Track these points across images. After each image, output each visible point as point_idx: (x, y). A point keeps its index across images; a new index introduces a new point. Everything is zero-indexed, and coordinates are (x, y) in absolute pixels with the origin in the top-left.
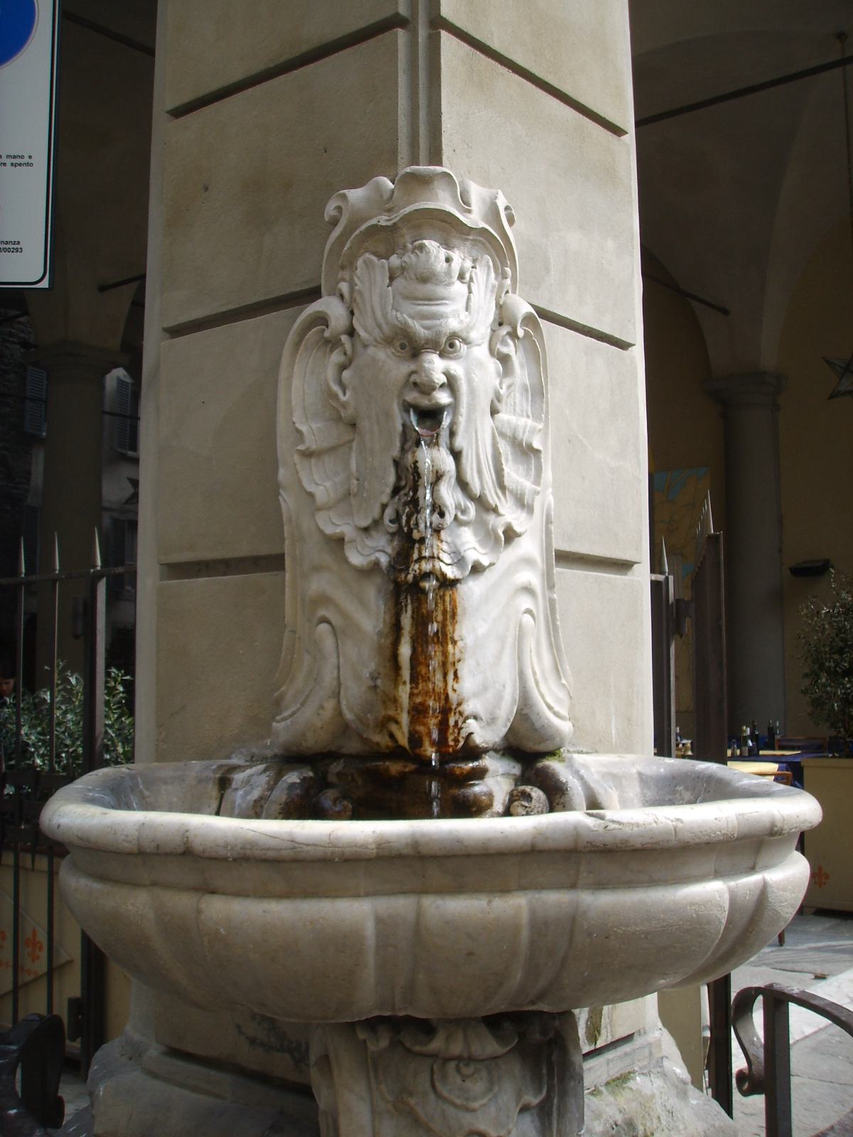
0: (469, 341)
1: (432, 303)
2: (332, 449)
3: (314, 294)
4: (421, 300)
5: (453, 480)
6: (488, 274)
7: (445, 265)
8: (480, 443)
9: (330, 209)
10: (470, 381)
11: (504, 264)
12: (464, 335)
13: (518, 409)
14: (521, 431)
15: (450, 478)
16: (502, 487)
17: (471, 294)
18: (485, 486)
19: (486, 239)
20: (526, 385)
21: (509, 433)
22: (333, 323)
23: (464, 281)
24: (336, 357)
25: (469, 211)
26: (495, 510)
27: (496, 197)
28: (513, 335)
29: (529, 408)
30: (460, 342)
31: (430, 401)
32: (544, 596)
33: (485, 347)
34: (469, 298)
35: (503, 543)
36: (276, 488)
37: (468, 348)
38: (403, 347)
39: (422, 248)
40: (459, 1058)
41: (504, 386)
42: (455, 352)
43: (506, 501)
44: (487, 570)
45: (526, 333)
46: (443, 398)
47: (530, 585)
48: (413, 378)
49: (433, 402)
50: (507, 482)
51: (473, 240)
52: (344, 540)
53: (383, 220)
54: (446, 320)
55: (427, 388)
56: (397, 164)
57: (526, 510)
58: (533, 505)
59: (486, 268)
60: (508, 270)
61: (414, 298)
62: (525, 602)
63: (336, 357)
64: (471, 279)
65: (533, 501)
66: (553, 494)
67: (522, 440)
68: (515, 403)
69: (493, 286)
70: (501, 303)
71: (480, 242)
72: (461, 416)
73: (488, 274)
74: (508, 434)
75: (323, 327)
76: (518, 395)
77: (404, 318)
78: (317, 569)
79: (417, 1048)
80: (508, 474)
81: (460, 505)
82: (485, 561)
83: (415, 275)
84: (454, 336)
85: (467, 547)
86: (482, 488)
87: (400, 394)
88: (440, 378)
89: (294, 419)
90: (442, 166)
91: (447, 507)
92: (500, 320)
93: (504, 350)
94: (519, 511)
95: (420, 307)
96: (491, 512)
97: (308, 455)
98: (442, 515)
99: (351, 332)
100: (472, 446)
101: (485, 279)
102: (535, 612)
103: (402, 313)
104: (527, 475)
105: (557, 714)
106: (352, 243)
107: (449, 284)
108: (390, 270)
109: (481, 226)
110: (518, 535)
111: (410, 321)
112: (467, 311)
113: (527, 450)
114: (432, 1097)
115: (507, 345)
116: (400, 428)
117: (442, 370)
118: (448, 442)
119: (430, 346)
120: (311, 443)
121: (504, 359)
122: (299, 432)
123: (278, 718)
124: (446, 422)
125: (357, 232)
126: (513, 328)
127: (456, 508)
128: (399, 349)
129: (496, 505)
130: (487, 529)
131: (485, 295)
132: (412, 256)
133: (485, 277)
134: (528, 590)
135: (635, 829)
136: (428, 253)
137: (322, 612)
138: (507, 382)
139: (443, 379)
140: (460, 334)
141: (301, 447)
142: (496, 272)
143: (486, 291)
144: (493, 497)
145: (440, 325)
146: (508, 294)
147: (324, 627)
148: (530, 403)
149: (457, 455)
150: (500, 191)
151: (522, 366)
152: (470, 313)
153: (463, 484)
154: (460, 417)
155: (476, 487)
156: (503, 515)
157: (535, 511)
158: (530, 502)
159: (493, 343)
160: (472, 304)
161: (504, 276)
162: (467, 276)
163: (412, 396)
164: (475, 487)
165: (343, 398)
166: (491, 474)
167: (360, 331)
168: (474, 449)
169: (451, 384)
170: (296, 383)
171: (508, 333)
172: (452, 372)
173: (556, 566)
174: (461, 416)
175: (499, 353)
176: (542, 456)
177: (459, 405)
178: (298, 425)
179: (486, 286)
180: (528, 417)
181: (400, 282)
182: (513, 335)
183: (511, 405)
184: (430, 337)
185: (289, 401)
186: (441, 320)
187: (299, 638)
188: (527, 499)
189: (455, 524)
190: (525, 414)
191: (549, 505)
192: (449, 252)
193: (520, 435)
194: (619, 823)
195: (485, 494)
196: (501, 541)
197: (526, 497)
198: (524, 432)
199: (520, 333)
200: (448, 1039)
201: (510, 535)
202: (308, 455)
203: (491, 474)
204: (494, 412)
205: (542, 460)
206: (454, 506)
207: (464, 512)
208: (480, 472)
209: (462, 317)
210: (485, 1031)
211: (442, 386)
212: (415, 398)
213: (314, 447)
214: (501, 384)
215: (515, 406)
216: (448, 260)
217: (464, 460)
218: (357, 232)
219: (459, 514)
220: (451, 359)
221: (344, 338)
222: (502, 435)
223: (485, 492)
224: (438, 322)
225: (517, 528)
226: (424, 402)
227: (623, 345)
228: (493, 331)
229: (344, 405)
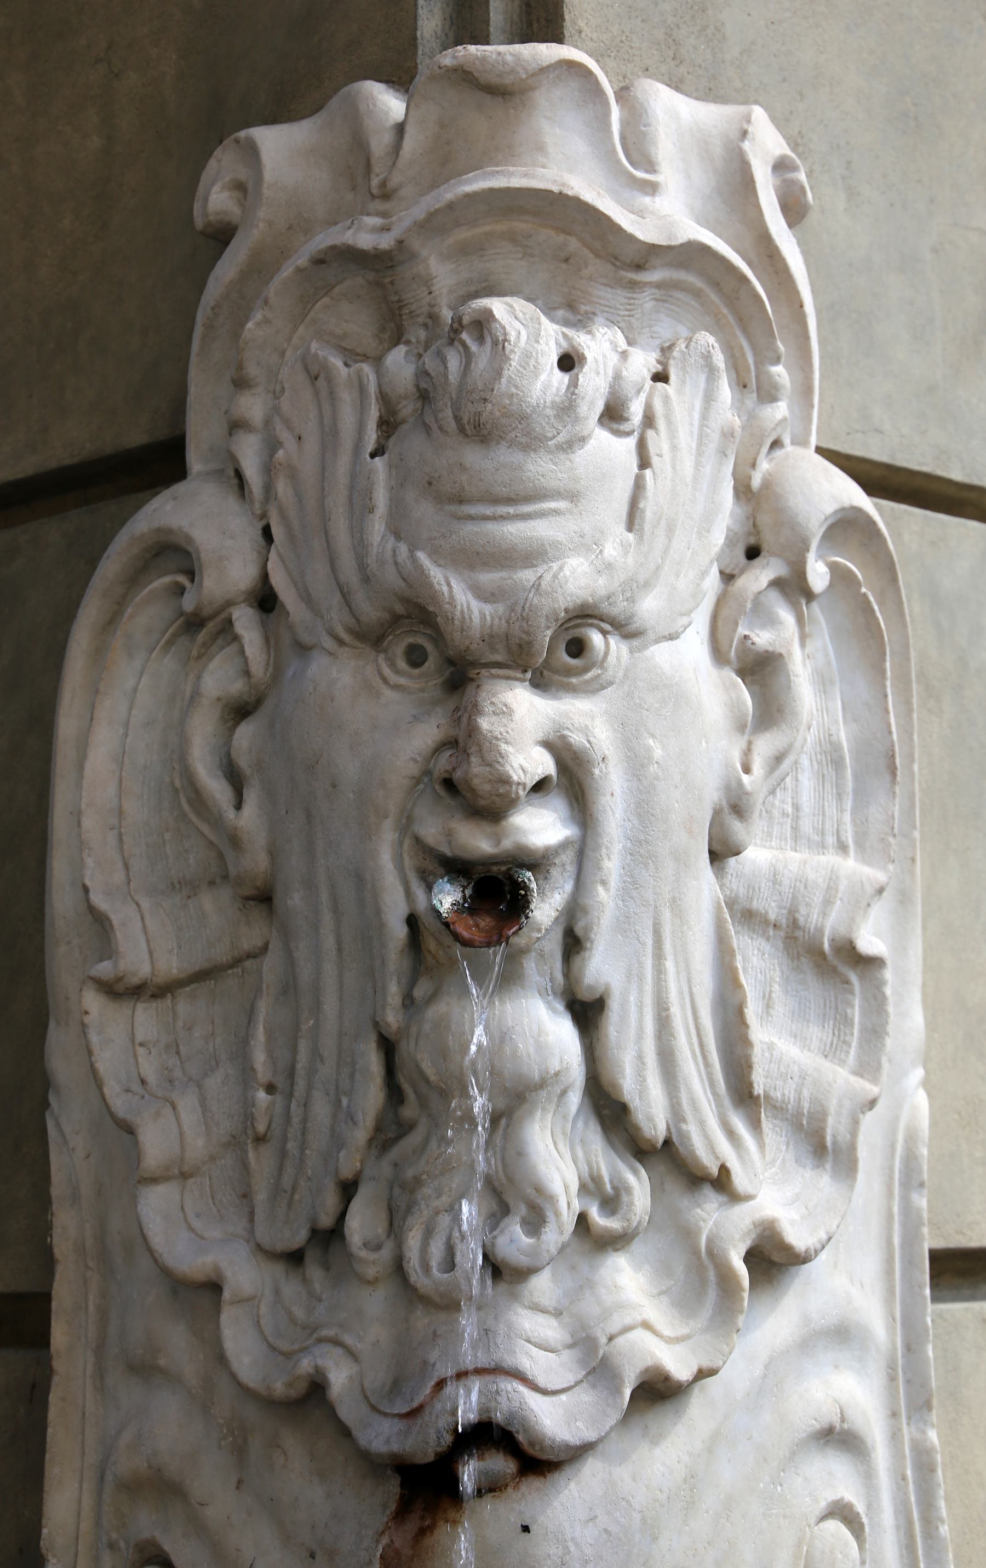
0: (633, 627)
1: (511, 510)
5: (575, 1099)
6: (709, 397)
7: (560, 379)
8: (669, 965)
11: (767, 355)
12: (618, 608)
13: (806, 825)
14: (818, 899)
15: (564, 1093)
17: (648, 472)
19: (702, 274)
20: (835, 748)
21: (773, 910)
23: (625, 427)
25: (652, 188)
27: (744, 133)
29: (847, 817)
30: (604, 633)
32: (895, 1436)
34: (639, 486)
35: (746, 1295)
37: (631, 651)
41: (758, 767)
42: (586, 669)
43: (761, 1145)
44: (696, 1389)
45: (834, 569)
47: (843, 1420)
49: (507, 844)
50: (760, 1083)
51: (660, 285)
54: (555, 566)
57: (828, 1166)
58: (853, 1147)
59: (702, 379)
60: (779, 371)
64: (649, 421)
65: (854, 1133)
66: (926, 1084)
67: (820, 931)
68: (797, 807)
69: (724, 435)
70: (756, 482)
72: (604, 883)
73: (709, 397)
74: (772, 916)
76: (807, 782)
77: (414, 560)
80: (771, 1047)
81: (596, 1179)
82: (681, 1371)
83: (457, 419)
85: (614, 1325)
86: (676, 1114)
87: (406, 824)
90: (557, 37)
91: (552, 1199)
92: (752, 540)
93: (763, 639)
94: (808, 1173)
96: (708, 1191)
98: (535, 1222)
100: (641, 978)
101: (696, 416)
102: (860, 1508)
104: (832, 1052)
107: (571, 445)
111: (436, 574)
112: (630, 527)
113: (836, 962)
115: (771, 621)
117: (540, 736)
118: (559, 977)
119: (499, 658)
126: (790, 564)
128: (402, 664)
129: (724, 1170)
130: (695, 1252)
131: (698, 465)
133: (698, 404)
136: (499, 346)
138: (765, 745)
139: (543, 764)
140: (605, 608)
142: (741, 384)
143: (700, 453)
145: (537, 586)
146: (778, 453)
148: (849, 804)
150: (758, 113)
151: (822, 682)
152: (641, 538)
154: (600, 889)
156: (749, 1198)
157: (861, 1165)
158: (844, 1137)
159: (725, 613)
160: (649, 507)
161: (768, 394)
162: (636, 410)
164: (650, 1119)
166: (707, 1064)
168: (649, 987)
171: (777, 583)
172: (576, 739)
173: (935, 1299)
174: (604, 883)
176: (888, 974)
177: (597, 848)
179: (702, 439)
180: (842, 848)
183: (785, 815)
186: (540, 570)
188: (835, 1127)
190: (831, 840)
191: (912, 1138)
192: (570, 332)
193: (811, 917)
195: (685, 1136)
196: (741, 1289)
197: (831, 1121)
198: (828, 902)
203: (707, 1064)
205: (888, 991)
206: (574, 1186)
207: (611, 1204)
209: (611, 551)
211: (540, 786)
215: (797, 818)
216: (568, 362)
219: (594, 1213)
220: (573, 690)
223: (684, 1127)
224: (527, 576)
228: (728, 577)
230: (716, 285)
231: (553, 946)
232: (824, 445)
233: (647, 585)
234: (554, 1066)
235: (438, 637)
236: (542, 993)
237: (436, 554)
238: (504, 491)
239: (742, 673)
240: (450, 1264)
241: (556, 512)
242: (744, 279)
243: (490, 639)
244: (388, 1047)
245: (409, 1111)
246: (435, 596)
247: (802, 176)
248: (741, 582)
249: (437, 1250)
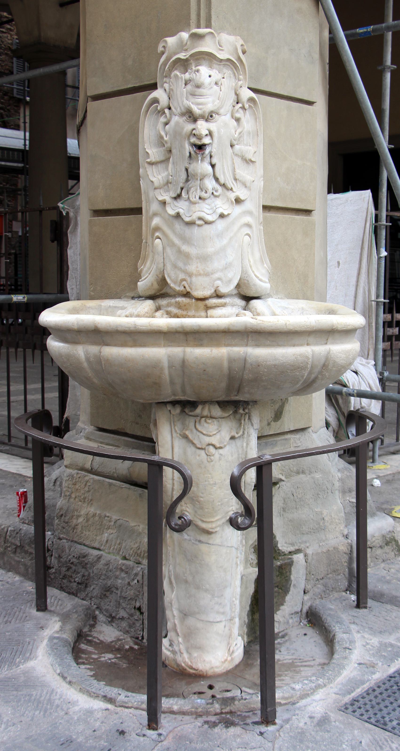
2: (161, 162)
3: (154, 87)
4: (198, 96)
9: (160, 49)
10: (219, 132)
16: (236, 179)
18: (227, 180)
20: (249, 131)
22: (161, 103)
24: (163, 119)
26: (231, 189)
28: (243, 108)
31: (201, 142)
33: (229, 115)
36: (138, 178)
38: (190, 117)
39: (198, 71)
40: (206, 417)
41: (237, 133)
45: (249, 106)
46: (206, 140)
48: (194, 132)
49: (202, 143)
52: (165, 203)
53: (182, 56)
55: (200, 138)
56: (190, 25)
61: (193, 95)
62: (247, 230)
63: (163, 119)
64: (221, 84)
71: (227, 65)
75: (157, 104)
78: (155, 214)
79: (190, 413)
81: (215, 188)
82: (226, 213)
84: (212, 112)
86: (225, 180)
88: (204, 132)
89: (145, 147)
91: (208, 190)
95: (197, 99)
97: (151, 164)
99: (170, 108)
102: (251, 235)
103: (189, 102)
105: (261, 280)
106: (169, 66)
108: (185, 80)
109: (227, 57)
110: (243, 201)
114: (195, 431)
116: (188, 154)
120: (152, 158)
121: (238, 120)
122: (147, 153)
123: (140, 280)
124: (207, 151)
125: (171, 60)
127: (212, 189)
132: (194, 75)
134: (248, 225)
135: (269, 323)
137: (157, 234)
139: (207, 132)
140: (215, 111)
141: (148, 160)
144: (230, 183)
147: (158, 241)
149: (213, 166)
153: (217, 180)
155: (222, 181)
163: (193, 140)
165: (165, 139)
167: (173, 108)
169: (210, 134)
170: (146, 131)
171: (240, 107)
175: (235, 118)
178: (147, 150)
180: (250, 146)
181: (189, 87)
182: (243, 108)
184: (201, 113)
185: (143, 138)
187: (149, 245)
188: (248, 184)
189: (212, 196)
192: (210, 72)
194: (263, 321)
199: (247, 106)
200: (203, 409)
201: (238, 201)
202: (151, 164)
204: (232, 146)
206: (211, 189)
207: (216, 191)
208: (224, 173)
210: (217, 406)
211: (206, 135)
212: (194, 141)
213: (154, 160)
214: (235, 132)
217: (217, 168)
218: (171, 60)
221: (167, 111)
222: (236, 155)
225: (242, 197)
226: (199, 143)
227: (310, 103)
229: (166, 142)
230: (231, 64)
231: (209, 157)
232: (249, 87)
233: (221, 108)
234: (208, 172)
235: (193, 115)
236: (207, 163)
237: (192, 103)
238: (202, 94)
239: (235, 120)
240: (195, 197)
241: (208, 98)
242: (235, 63)
243: (199, 115)
244: (187, 170)
245: (189, 178)
246: (192, 109)
247: (245, 47)
248: (235, 107)
249: (194, 196)
